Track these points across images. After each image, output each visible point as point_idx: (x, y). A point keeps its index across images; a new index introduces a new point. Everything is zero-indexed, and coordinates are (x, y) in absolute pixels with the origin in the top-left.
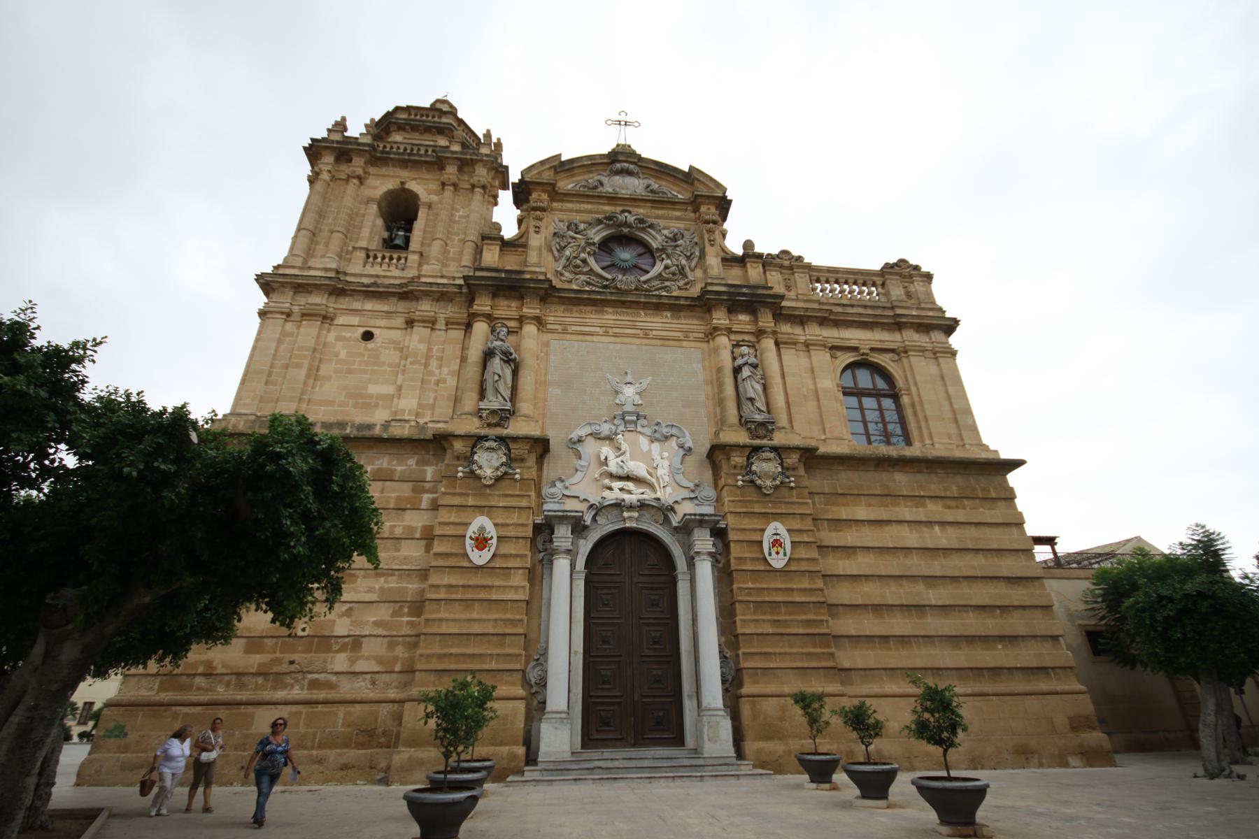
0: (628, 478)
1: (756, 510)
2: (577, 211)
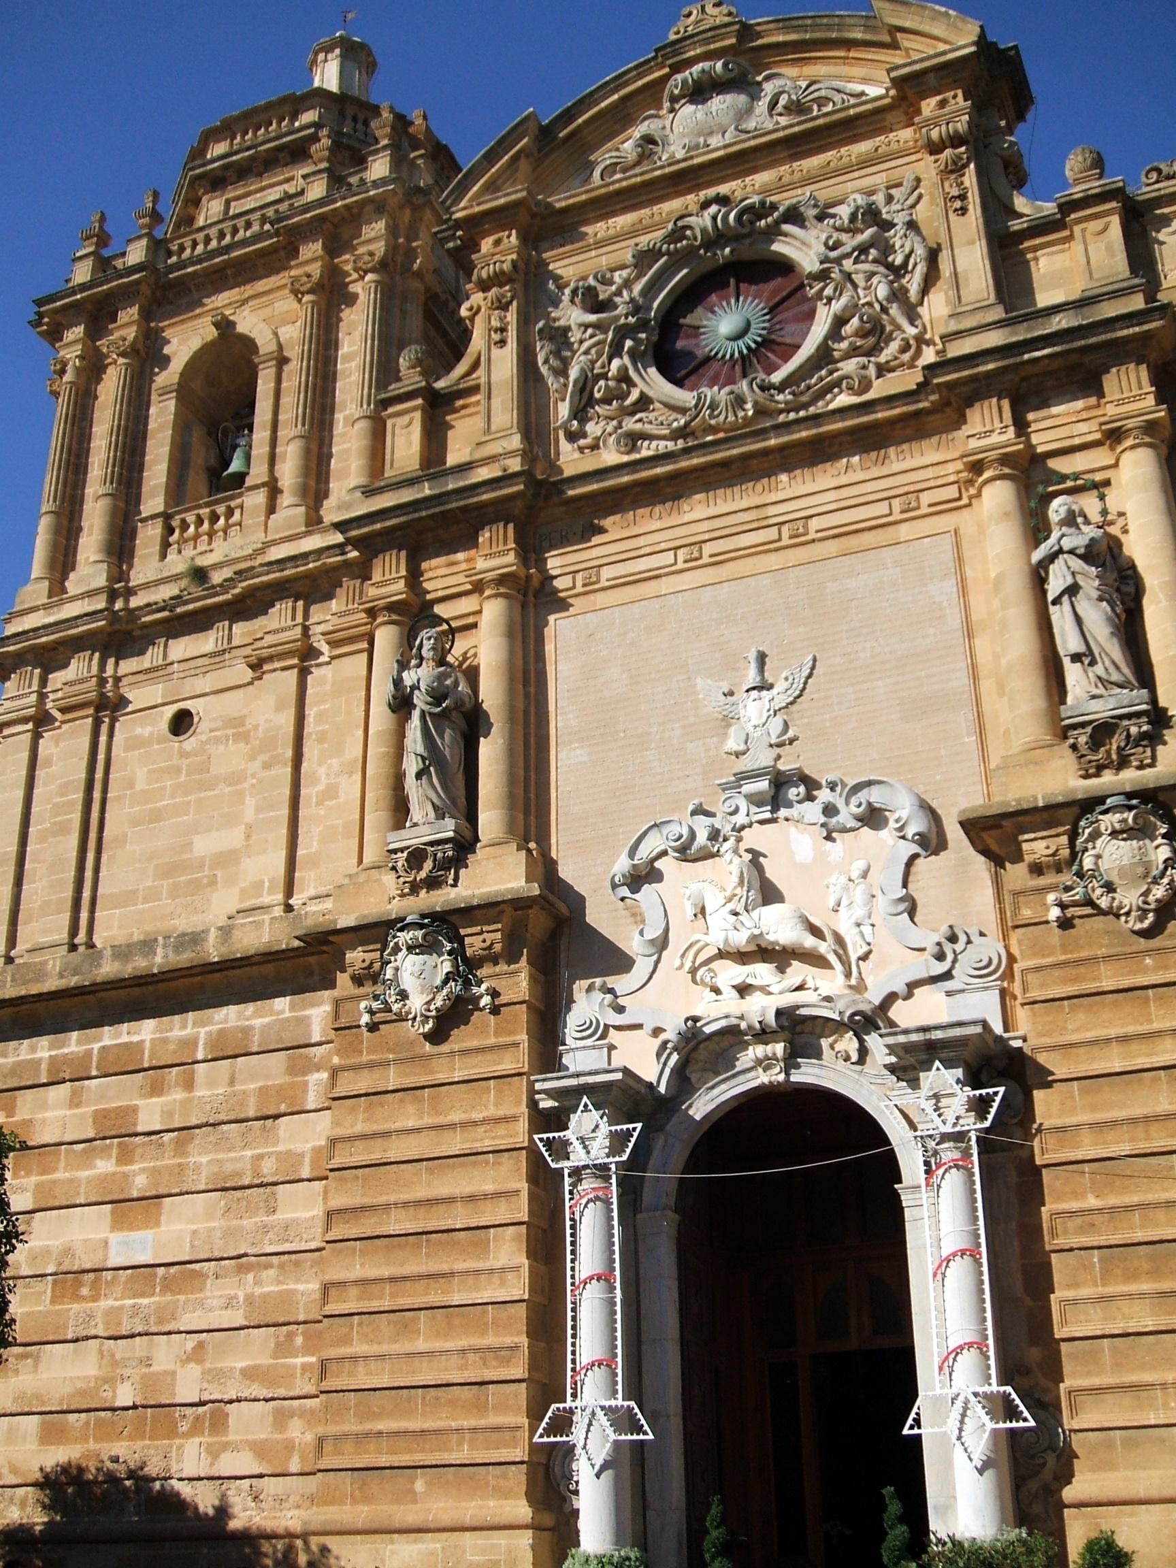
1: (1108, 985)
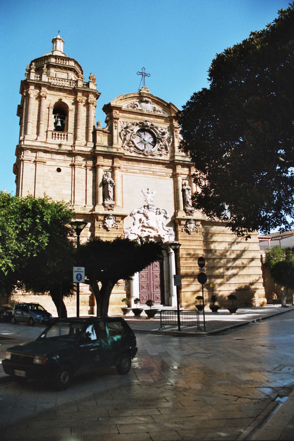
0: (150, 228)
1: (187, 239)
2: (129, 118)
